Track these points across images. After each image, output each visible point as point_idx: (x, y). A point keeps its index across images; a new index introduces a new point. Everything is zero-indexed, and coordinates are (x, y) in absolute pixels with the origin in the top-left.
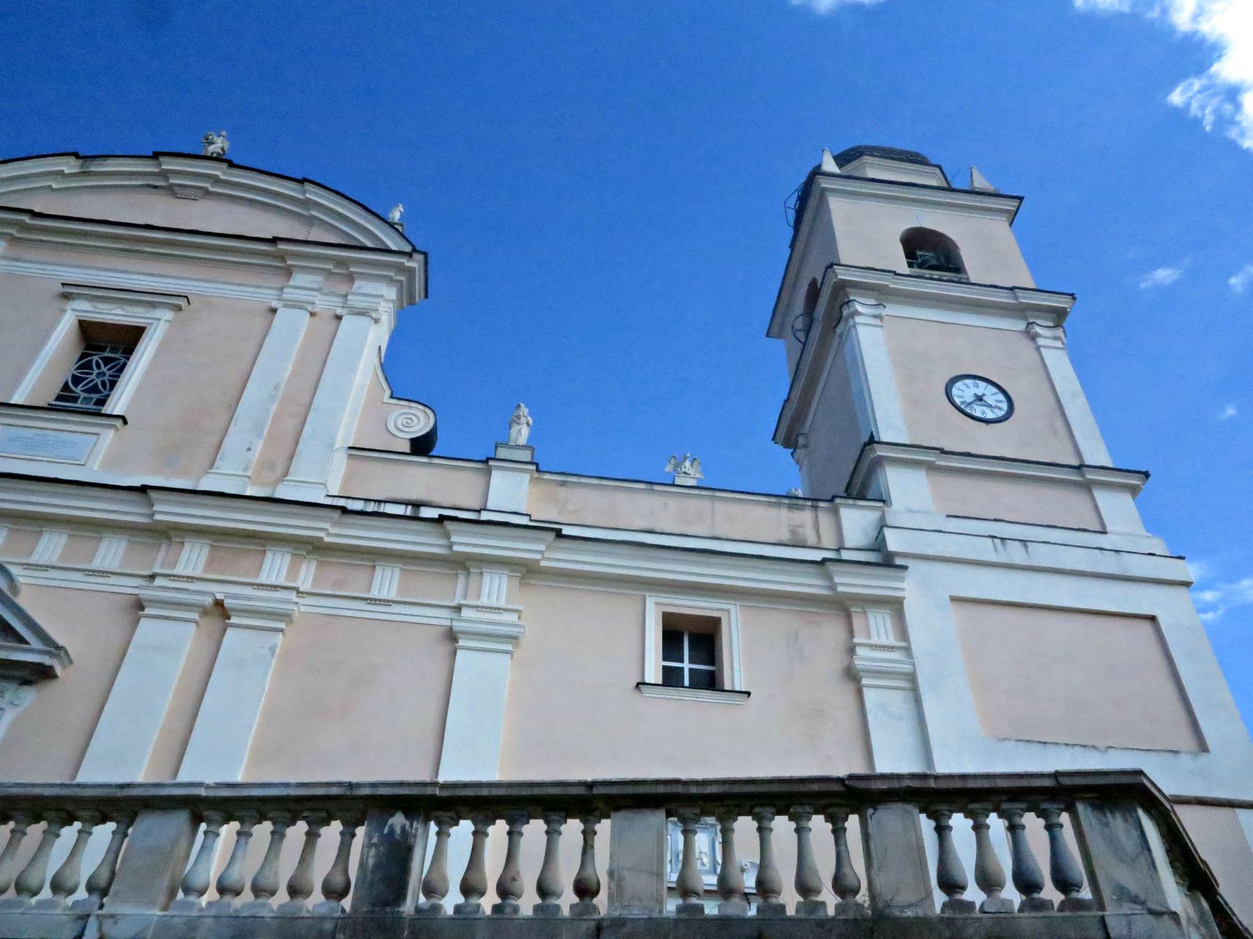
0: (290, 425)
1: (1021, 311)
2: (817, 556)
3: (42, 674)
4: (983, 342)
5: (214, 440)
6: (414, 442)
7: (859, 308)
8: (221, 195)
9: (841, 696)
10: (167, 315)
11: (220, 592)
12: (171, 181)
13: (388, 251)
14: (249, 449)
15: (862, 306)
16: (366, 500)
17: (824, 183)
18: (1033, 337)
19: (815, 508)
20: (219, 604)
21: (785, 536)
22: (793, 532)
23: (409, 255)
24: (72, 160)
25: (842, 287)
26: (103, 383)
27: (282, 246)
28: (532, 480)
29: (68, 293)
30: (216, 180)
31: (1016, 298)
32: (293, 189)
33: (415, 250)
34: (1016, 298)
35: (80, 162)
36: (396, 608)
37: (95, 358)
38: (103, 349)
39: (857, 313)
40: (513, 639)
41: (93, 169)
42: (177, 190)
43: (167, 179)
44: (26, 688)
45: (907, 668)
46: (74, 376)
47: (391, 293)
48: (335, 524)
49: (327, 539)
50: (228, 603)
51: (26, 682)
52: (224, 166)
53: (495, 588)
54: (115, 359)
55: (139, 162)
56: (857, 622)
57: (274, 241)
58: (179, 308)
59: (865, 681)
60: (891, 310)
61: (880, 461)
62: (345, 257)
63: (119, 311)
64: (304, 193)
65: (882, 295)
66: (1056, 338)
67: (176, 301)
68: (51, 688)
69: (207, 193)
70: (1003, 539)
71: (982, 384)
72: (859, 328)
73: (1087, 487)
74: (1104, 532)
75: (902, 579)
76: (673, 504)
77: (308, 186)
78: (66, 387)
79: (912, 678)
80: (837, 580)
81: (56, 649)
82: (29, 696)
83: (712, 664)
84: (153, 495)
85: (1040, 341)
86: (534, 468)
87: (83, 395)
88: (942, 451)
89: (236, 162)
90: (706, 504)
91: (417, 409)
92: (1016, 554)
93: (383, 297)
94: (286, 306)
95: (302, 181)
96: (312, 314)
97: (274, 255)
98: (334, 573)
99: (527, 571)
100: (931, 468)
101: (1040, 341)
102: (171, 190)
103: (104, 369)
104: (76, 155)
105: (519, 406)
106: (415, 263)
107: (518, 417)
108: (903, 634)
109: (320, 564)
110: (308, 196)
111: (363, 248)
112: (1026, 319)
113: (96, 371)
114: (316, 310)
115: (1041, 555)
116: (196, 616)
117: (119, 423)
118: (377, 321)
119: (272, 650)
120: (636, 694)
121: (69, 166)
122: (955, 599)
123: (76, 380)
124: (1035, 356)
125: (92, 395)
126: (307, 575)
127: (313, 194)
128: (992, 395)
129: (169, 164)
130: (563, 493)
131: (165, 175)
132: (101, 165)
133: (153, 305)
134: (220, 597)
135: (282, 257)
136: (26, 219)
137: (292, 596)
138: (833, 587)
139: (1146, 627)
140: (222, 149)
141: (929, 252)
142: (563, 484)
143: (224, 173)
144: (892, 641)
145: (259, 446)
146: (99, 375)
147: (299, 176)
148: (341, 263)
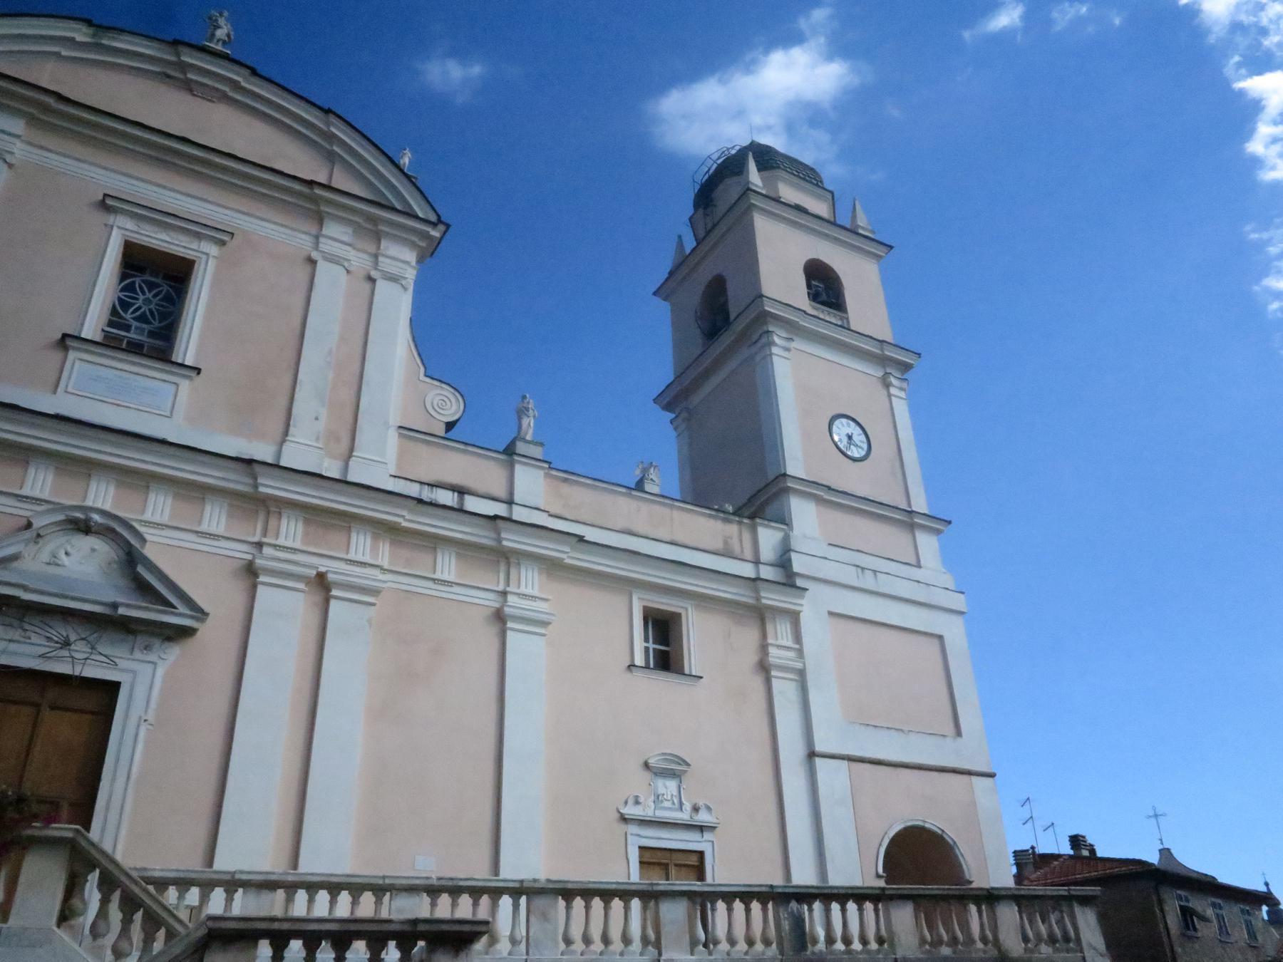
0: (347, 395)
1: (882, 361)
2: (747, 570)
3: (184, 633)
4: (853, 382)
5: (282, 402)
6: (450, 426)
7: (776, 339)
8: (236, 101)
9: (757, 683)
10: (213, 250)
11: (324, 565)
12: (190, 76)
13: (416, 217)
14: (317, 419)
15: (779, 337)
16: (421, 483)
17: (755, 201)
18: (887, 385)
19: (740, 523)
20: (321, 577)
21: (718, 545)
22: (726, 543)
23: (434, 225)
24: (85, 29)
25: (764, 317)
26: (150, 310)
27: (318, 191)
28: (547, 476)
29: (106, 204)
30: (236, 86)
31: (882, 350)
32: (316, 117)
33: (440, 221)
34: (882, 350)
35: (91, 31)
36: (456, 589)
37: (138, 281)
38: (141, 270)
39: (774, 343)
40: (545, 624)
41: (105, 42)
42: (193, 86)
43: (185, 74)
44: (167, 644)
45: (799, 665)
46: (120, 299)
47: (411, 256)
48: (410, 511)
49: (405, 524)
50: (331, 577)
51: (169, 639)
52: (246, 72)
53: (529, 581)
54: (158, 286)
55: (155, 44)
56: (770, 628)
57: (311, 183)
58: (222, 243)
59: (773, 673)
60: (797, 344)
61: (787, 490)
62: (376, 216)
63: (163, 236)
64: (328, 124)
65: (794, 329)
66: (901, 389)
67: (220, 235)
68: (191, 644)
69: (225, 98)
70: (863, 569)
71: (858, 430)
72: (775, 358)
73: (911, 527)
74: (919, 566)
75: (803, 597)
76: (645, 507)
77: (332, 118)
78: (114, 312)
79: (802, 673)
80: (763, 594)
81: (201, 614)
82: (173, 653)
83: (667, 645)
84: (257, 468)
85: (893, 391)
86: (546, 466)
87: (134, 324)
88: (829, 488)
89: (259, 69)
90: (666, 511)
91: (447, 391)
92: (868, 582)
93: (401, 258)
94: (326, 259)
95: (328, 111)
96: (348, 272)
97: (309, 200)
98: (405, 553)
99: (552, 567)
100: (819, 500)
101: (893, 391)
102: (188, 86)
103: (149, 295)
104: (89, 23)
105: (524, 397)
106: (435, 233)
107: (527, 409)
108: (798, 637)
109: (393, 543)
110: (333, 129)
111: (393, 209)
112: (884, 367)
113: (141, 297)
114: (351, 269)
115: (886, 585)
116: (301, 586)
117: (193, 374)
118: (405, 289)
119: (369, 621)
120: (629, 675)
121: (81, 34)
122: (831, 614)
123: (125, 305)
124: (887, 400)
125: (144, 326)
126: (384, 553)
127: (338, 130)
128: (859, 437)
129: (189, 58)
130: (566, 489)
131: (184, 67)
132: (114, 39)
133: (198, 236)
134: (322, 569)
135: (315, 200)
136: (51, 101)
137: (376, 572)
138: (758, 599)
139: (936, 641)
140: (228, 36)
141: (824, 285)
142: (566, 480)
143: (245, 79)
144: (790, 643)
145: (323, 413)
146: (147, 301)
147: (326, 107)
148: (373, 220)
